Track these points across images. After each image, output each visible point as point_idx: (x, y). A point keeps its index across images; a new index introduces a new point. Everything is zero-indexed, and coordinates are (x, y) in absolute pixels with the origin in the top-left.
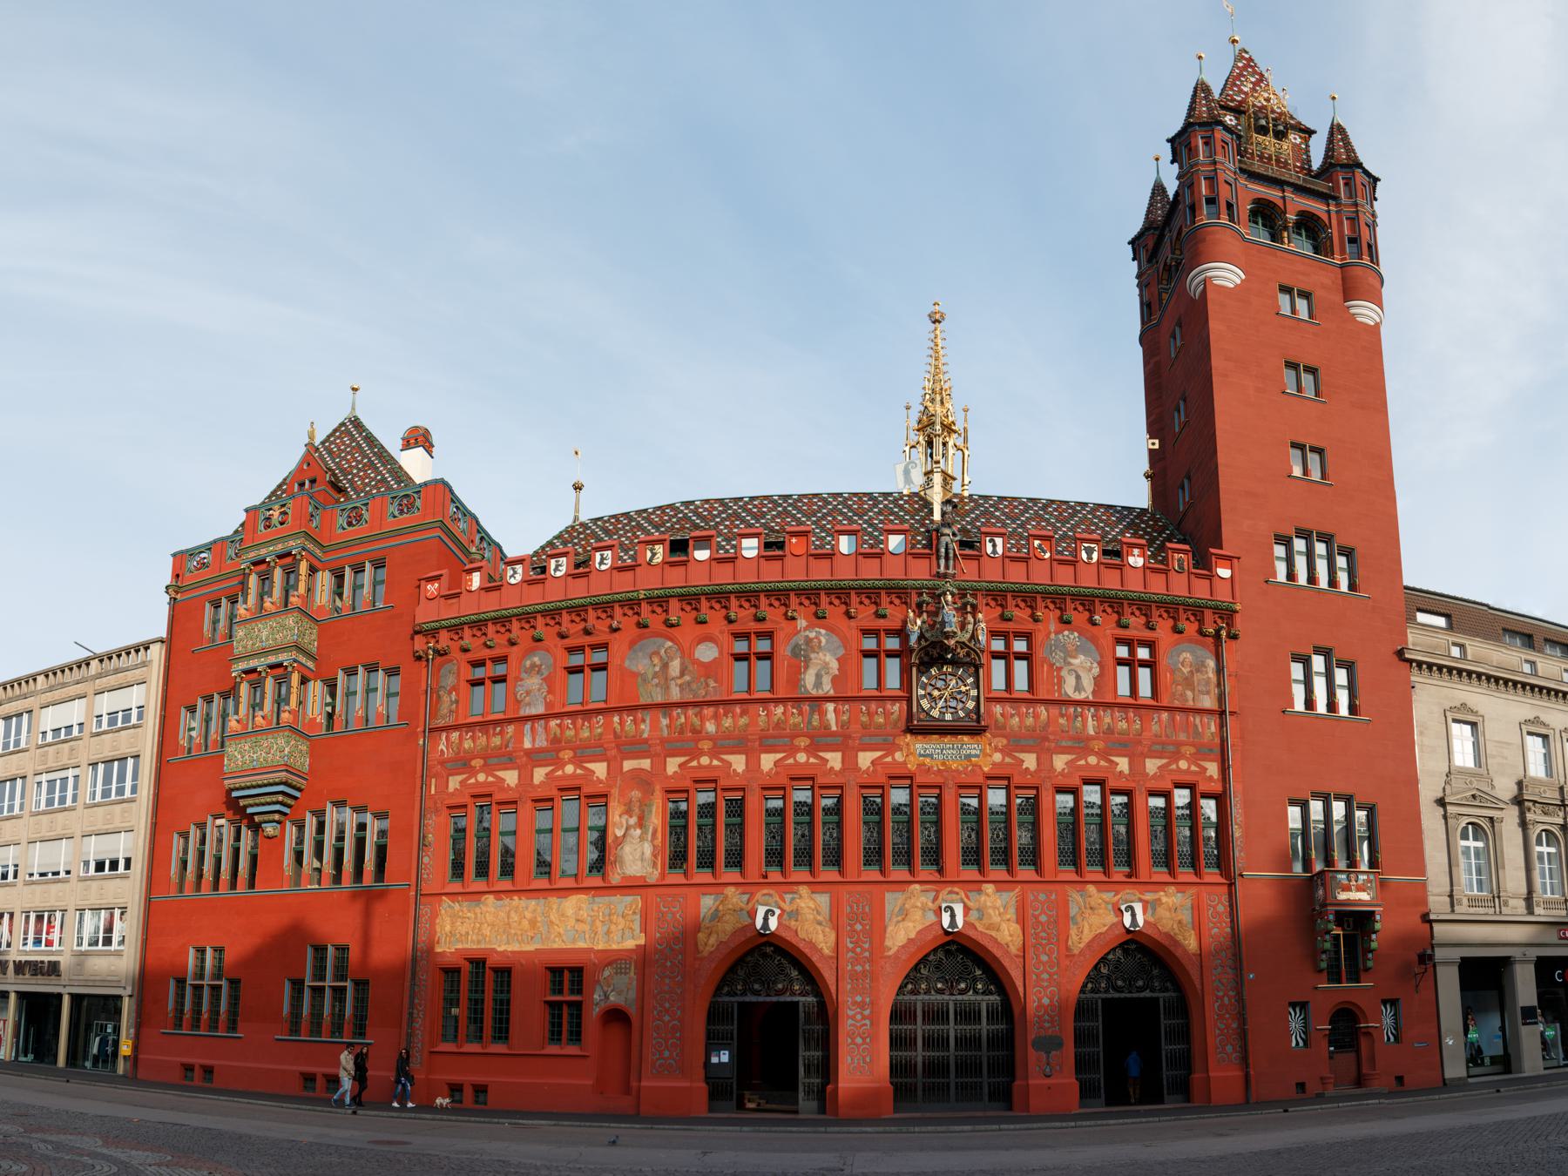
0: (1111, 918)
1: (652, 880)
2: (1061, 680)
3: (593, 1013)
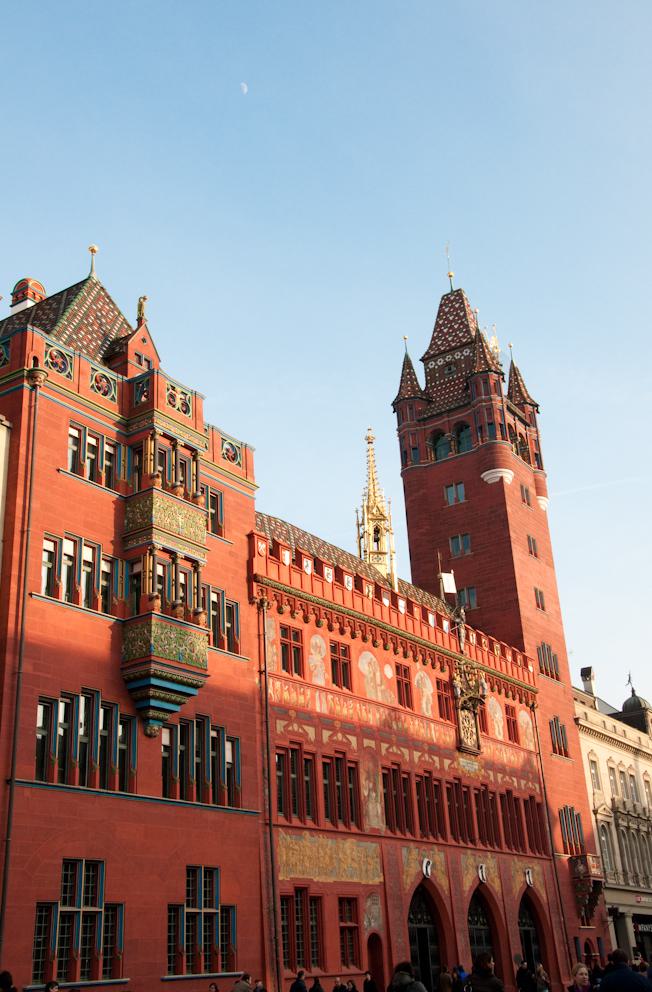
0: (523, 879)
1: (383, 834)
2: (494, 729)
3: (365, 937)
